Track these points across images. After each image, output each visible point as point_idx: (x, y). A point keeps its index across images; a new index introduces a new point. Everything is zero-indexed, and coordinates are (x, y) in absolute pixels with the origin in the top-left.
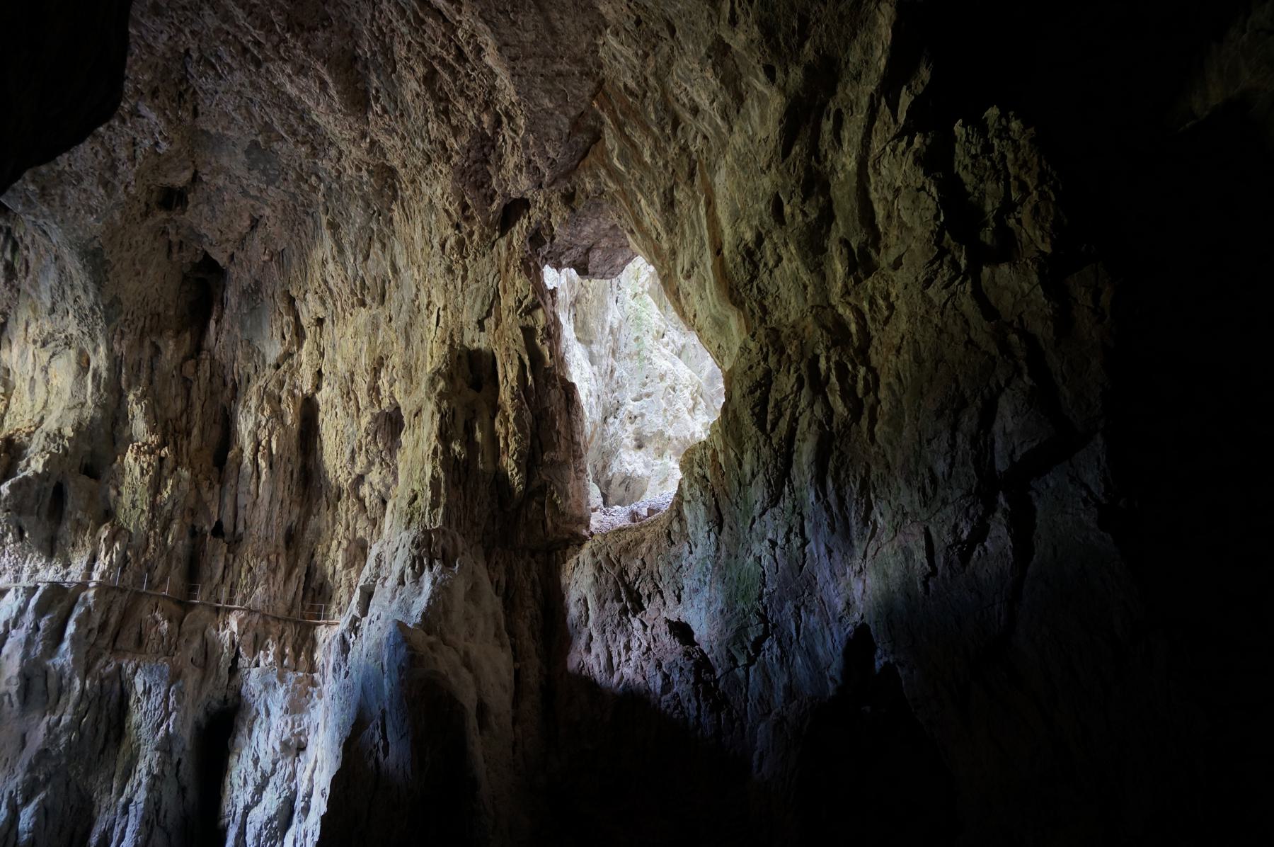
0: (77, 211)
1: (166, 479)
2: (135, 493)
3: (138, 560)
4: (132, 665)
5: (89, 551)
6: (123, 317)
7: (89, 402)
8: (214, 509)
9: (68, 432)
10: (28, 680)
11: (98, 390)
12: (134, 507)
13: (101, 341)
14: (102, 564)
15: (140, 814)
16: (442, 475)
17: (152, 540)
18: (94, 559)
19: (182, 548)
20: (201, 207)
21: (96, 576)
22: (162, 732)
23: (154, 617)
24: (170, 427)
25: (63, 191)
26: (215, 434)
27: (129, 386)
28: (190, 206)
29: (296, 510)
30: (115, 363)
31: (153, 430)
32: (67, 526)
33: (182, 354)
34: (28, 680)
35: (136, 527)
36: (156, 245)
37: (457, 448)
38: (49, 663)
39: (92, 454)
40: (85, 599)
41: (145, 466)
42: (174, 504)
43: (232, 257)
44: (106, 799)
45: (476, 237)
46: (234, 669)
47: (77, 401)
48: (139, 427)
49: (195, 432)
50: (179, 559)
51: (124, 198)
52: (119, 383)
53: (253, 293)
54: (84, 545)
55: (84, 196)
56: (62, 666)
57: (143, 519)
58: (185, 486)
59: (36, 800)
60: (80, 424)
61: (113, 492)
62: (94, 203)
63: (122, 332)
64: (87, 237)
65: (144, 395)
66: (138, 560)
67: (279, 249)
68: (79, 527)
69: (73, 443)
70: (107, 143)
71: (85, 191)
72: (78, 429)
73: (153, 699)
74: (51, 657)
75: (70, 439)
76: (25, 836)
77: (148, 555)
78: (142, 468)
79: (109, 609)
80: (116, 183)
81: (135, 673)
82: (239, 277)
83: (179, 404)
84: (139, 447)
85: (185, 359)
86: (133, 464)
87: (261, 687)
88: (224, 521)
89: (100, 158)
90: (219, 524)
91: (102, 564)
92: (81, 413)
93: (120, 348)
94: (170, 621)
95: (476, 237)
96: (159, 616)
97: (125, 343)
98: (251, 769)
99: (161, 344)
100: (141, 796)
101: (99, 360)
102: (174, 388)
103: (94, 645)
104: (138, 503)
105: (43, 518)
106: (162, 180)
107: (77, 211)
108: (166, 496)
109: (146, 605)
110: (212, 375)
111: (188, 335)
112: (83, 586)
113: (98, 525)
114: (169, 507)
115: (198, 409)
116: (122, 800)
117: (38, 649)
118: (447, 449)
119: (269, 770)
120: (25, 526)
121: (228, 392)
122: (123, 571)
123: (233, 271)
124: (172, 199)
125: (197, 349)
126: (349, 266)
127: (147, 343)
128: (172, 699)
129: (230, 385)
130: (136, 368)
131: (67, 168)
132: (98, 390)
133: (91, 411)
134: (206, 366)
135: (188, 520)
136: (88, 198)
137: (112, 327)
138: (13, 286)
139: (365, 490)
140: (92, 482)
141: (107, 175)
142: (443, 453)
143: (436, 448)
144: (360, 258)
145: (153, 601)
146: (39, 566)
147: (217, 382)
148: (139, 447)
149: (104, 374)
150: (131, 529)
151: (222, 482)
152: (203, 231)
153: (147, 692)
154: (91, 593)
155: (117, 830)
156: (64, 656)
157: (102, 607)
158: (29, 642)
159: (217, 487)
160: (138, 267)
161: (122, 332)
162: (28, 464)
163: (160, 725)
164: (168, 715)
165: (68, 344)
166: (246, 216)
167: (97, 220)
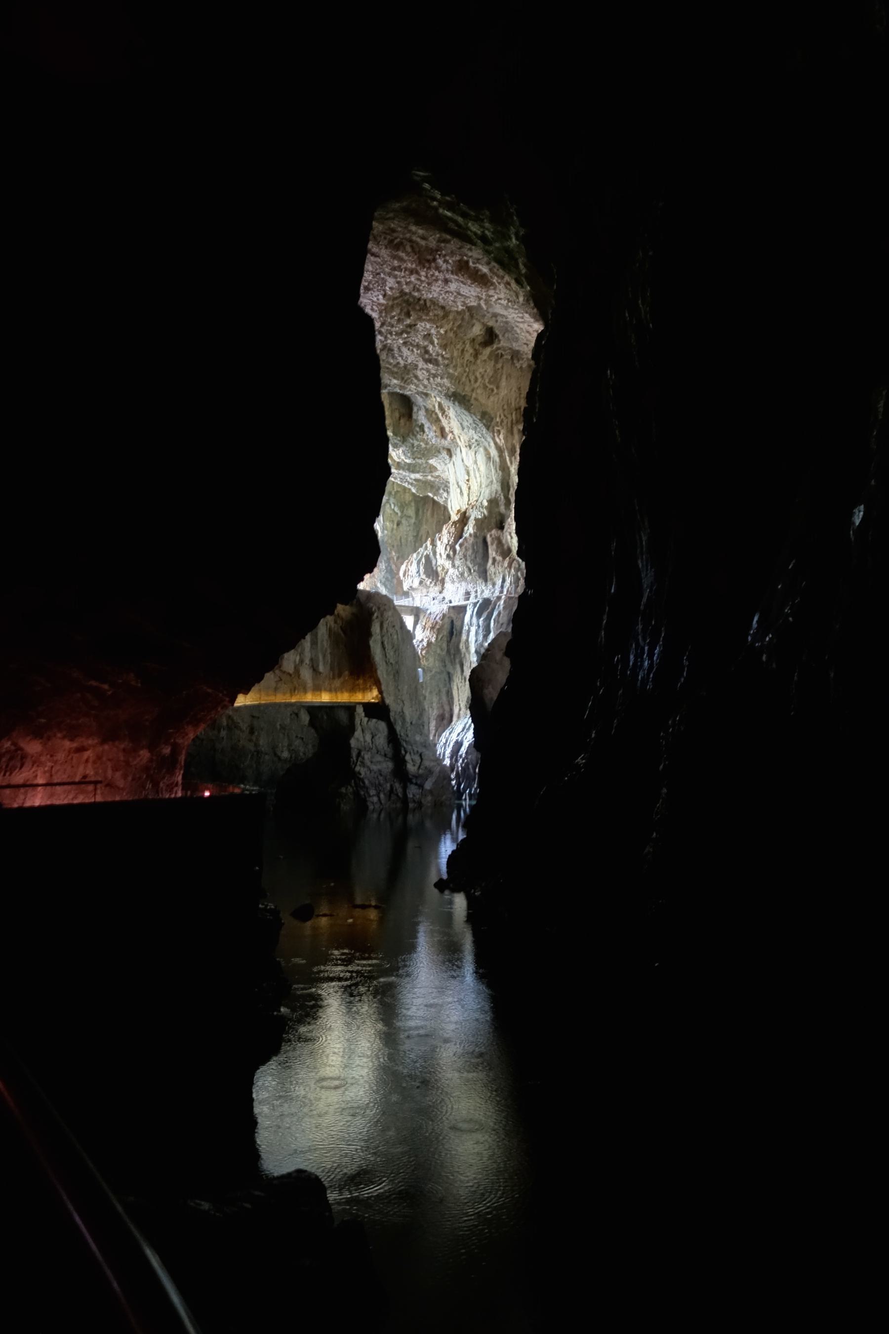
9: (485, 503)
18: (504, 581)
21: (505, 593)
28: (500, 337)
36: (499, 366)
75: (486, 508)
91: (507, 584)
97: (501, 436)
101: (494, 453)
112: (499, 598)
113: (504, 558)
117: (481, 638)
124: (490, 336)
140: (499, 532)
141: (427, 356)
154: (502, 602)
158: (477, 633)
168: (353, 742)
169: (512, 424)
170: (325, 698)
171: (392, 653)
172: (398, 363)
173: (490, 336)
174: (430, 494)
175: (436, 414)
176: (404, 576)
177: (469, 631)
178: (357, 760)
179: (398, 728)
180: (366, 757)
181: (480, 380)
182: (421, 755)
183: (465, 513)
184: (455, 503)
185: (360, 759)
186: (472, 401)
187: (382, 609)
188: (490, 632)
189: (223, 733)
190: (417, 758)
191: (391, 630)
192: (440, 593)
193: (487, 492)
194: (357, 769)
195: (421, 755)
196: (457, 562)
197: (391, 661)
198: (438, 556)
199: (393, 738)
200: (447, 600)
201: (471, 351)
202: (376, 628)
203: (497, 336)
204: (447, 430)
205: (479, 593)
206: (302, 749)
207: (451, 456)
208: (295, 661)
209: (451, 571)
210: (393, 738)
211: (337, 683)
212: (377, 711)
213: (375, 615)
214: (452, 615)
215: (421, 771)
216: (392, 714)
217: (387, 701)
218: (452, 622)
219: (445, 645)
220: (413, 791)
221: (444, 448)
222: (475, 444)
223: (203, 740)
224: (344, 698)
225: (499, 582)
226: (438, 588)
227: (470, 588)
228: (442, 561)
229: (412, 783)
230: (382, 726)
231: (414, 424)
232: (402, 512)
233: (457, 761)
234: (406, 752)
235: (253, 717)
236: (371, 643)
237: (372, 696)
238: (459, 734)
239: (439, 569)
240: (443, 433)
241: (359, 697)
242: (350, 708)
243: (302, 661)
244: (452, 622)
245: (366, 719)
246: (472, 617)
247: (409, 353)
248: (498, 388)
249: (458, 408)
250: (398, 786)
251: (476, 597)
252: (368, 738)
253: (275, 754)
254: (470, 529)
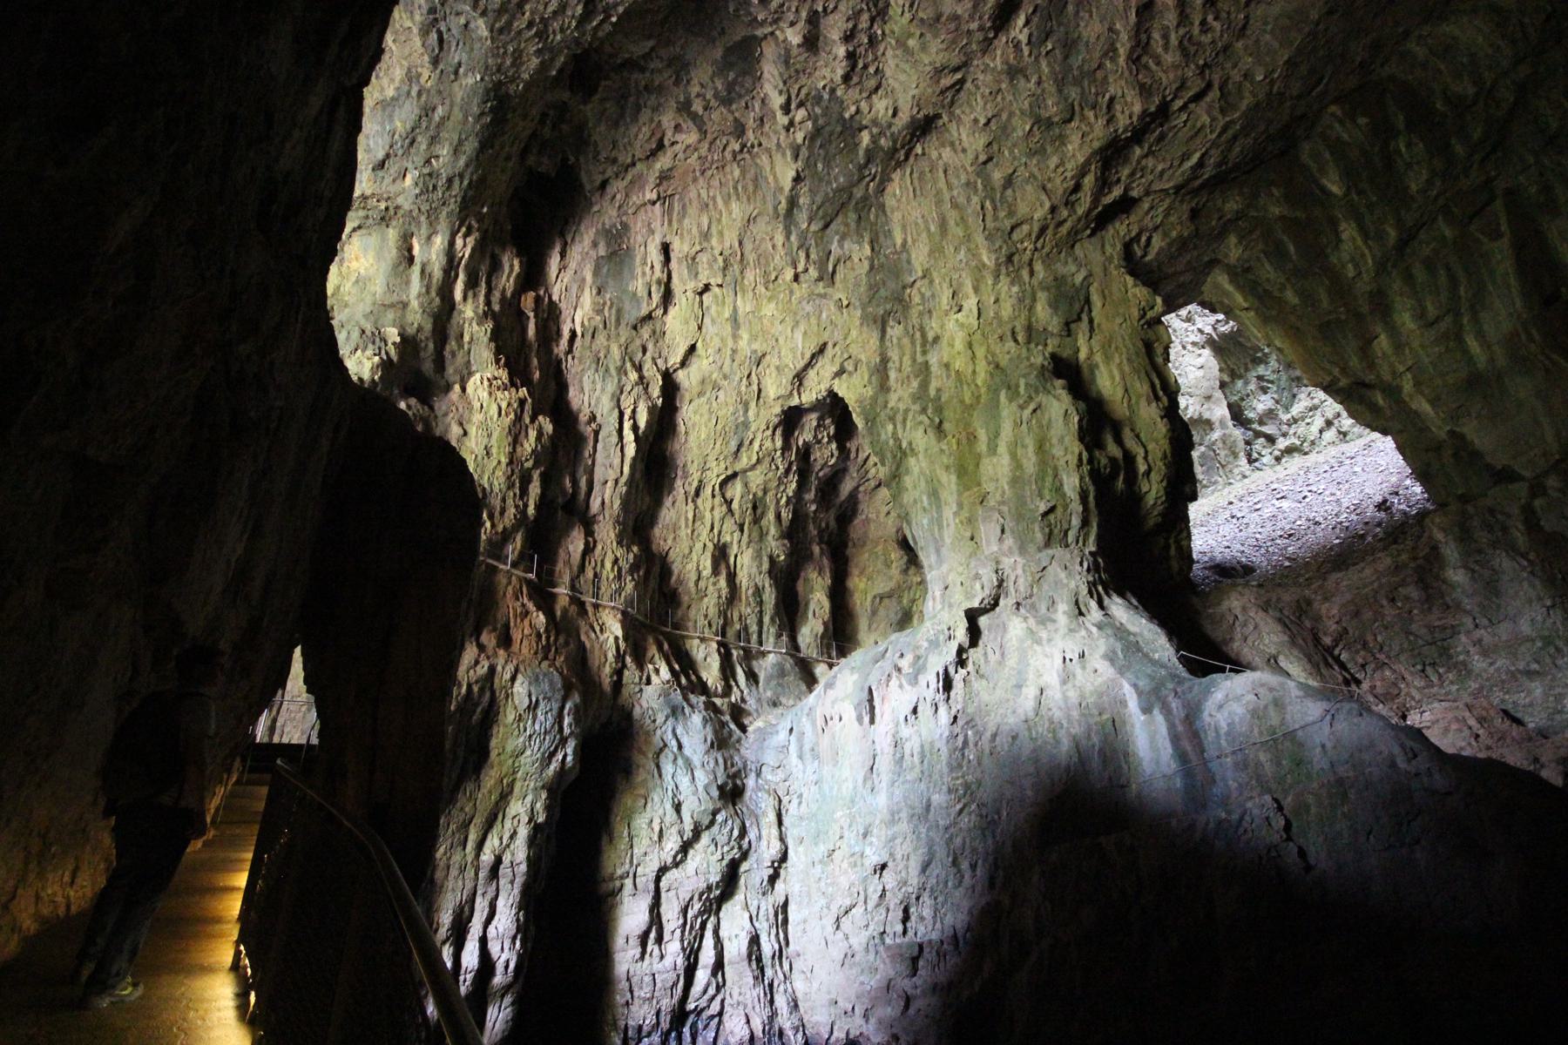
3: (493, 526)
4: (510, 668)
11: (428, 292)
15: (519, 881)
22: (554, 766)
28: (596, 97)
29: (647, 499)
41: (504, 405)
44: (457, 858)
45: (1064, 230)
46: (618, 685)
47: (395, 298)
52: (451, 292)
73: (541, 717)
81: (513, 679)
87: (667, 711)
93: (465, 247)
95: (1064, 230)
97: (471, 241)
98: (671, 815)
100: (519, 852)
104: (494, 451)
116: (487, 857)
119: (706, 822)
121: (564, 342)
128: (567, 721)
133: (418, 316)
139: (736, 490)
143: (1080, 454)
153: (533, 708)
155: (481, 905)
163: (552, 754)
164: (563, 741)
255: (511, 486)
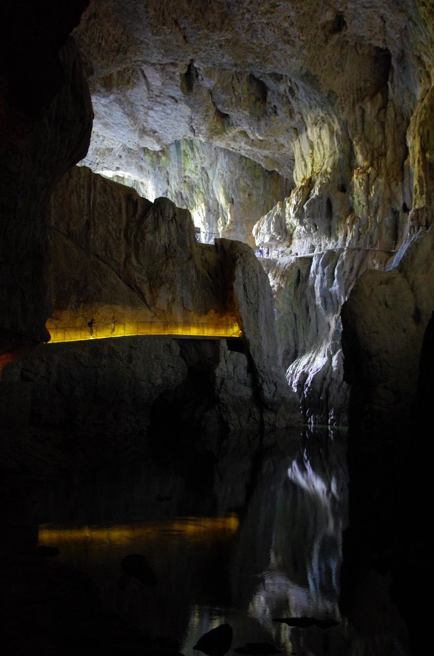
0: (285, 60)
1: (371, 186)
2: (358, 197)
5: (343, 231)
6: (339, 99)
7: (337, 151)
8: (400, 197)
9: (329, 170)
10: (325, 298)
12: (360, 204)
13: (334, 116)
14: (349, 238)
16: (423, 174)
17: (369, 220)
18: (346, 235)
19: (388, 220)
20: (353, 22)
21: (347, 245)
23: (373, 262)
24: (376, 154)
25: (273, 54)
26: (400, 150)
27: (353, 136)
30: (344, 125)
31: (365, 159)
32: (334, 219)
33: (377, 107)
34: (325, 298)
35: (362, 214)
36: (344, 52)
37: (428, 156)
38: (330, 289)
39: (342, 178)
40: (342, 256)
41: (361, 180)
42: (378, 199)
43: (384, 41)
47: (332, 151)
48: (360, 158)
49: (389, 153)
50: (388, 229)
51: (302, 43)
53: (402, 58)
54: (341, 229)
55: (282, 52)
56: (335, 291)
57: (364, 210)
58: (381, 187)
59: (337, 353)
60: (334, 164)
61: (351, 198)
62: (289, 53)
63: (342, 108)
64: (298, 69)
65: (360, 139)
66: (364, 233)
67: (403, 27)
68: (340, 219)
69: (332, 175)
70: (275, 24)
71: (282, 49)
72: (333, 168)
74: (331, 287)
75: (330, 174)
76: (335, 369)
77: (368, 230)
78: (360, 183)
79: (353, 261)
80: (293, 39)
82: (394, 50)
83: (380, 138)
84: (358, 170)
85: (379, 110)
86: (357, 180)
88: (406, 202)
89: (277, 32)
90: (405, 205)
91: (349, 238)
92: (334, 158)
94: (381, 263)
96: (375, 261)
99: (364, 106)
101: (336, 127)
102: (376, 129)
103: (347, 279)
105: (324, 217)
106: (319, 22)
107: (285, 60)
108: (372, 195)
109: (370, 256)
110: (396, 115)
111: (379, 96)
112: (342, 250)
113: (347, 217)
114: (375, 201)
115: (390, 138)
117: (325, 284)
118: (424, 158)
120: (317, 224)
122: (358, 240)
123: (389, 48)
124: (339, 24)
125: (386, 101)
126: (422, 31)
127: (357, 108)
129: (405, 119)
130: (354, 125)
131: (267, 44)
132: (340, 143)
133: (338, 155)
134: (391, 113)
135: (388, 206)
136: (285, 52)
137: (336, 106)
138: (296, 98)
140: (343, 194)
141: (286, 37)
142: (423, 161)
143: (419, 158)
144: (424, 26)
145: (373, 254)
146: (327, 242)
147: (399, 118)
148: (358, 170)
149: (340, 133)
150: (360, 216)
151: (403, 180)
152: (361, 35)
156: (335, 286)
157: (350, 260)
158: (322, 281)
159: (400, 183)
160: (337, 69)
161: (342, 108)
162: (314, 192)
165: (324, 121)
166: (376, 17)
167: (297, 59)
168: (217, 372)
169: (354, 103)
170: (194, 332)
171: (252, 295)
172: (261, 44)
173: (339, 24)
174: (277, 170)
175: (287, 97)
176: (257, 234)
177: (315, 277)
178: (221, 388)
179: (256, 360)
180: (229, 384)
181: (328, 63)
182: (275, 385)
183: (310, 179)
184: (299, 176)
185: (223, 387)
186: (321, 82)
187: (244, 256)
188: (334, 279)
189: (104, 361)
190: (273, 388)
191: (251, 274)
192: (288, 247)
193: (331, 160)
194: (220, 396)
195: (275, 385)
196: (305, 220)
197: (252, 301)
198: (287, 216)
199: (252, 368)
200: (293, 253)
201: (322, 37)
202: (238, 273)
203: (344, 23)
204: (296, 110)
205: (323, 247)
206: (173, 377)
207: (297, 135)
208: (168, 300)
209: (298, 228)
210: (252, 368)
211: (204, 319)
212: (237, 345)
213: (238, 260)
214: (299, 265)
215: (275, 398)
216: (251, 347)
217: (248, 336)
218: (299, 271)
219: (292, 291)
220: (269, 417)
221: (291, 127)
222: (321, 121)
223: (86, 367)
224: (209, 332)
225: (341, 237)
226: (287, 243)
227: (315, 242)
228: (291, 219)
229: (268, 408)
230: (243, 358)
231: (268, 105)
232: (253, 185)
233: (303, 390)
234: (263, 381)
235: (131, 347)
236: (234, 284)
237: (234, 331)
238: (304, 367)
239: (288, 227)
240: (291, 113)
241: (222, 333)
242: (214, 342)
243: (173, 300)
244: (299, 271)
245: (229, 352)
246: (317, 266)
247: (272, 34)
248: (343, 70)
249: (309, 88)
250: (255, 409)
251: (320, 250)
252: (231, 367)
253: (150, 380)
254: (316, 192)
255: (368, 213)
